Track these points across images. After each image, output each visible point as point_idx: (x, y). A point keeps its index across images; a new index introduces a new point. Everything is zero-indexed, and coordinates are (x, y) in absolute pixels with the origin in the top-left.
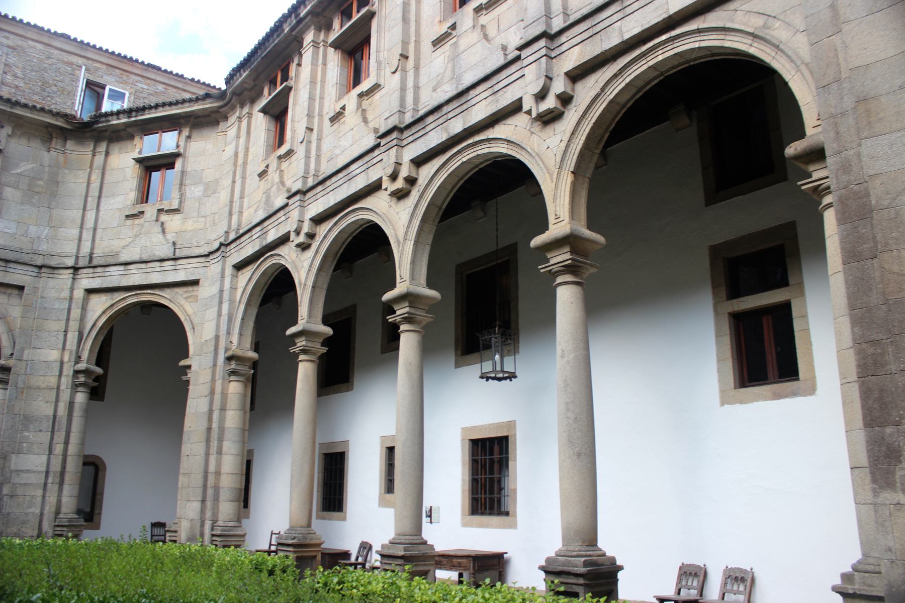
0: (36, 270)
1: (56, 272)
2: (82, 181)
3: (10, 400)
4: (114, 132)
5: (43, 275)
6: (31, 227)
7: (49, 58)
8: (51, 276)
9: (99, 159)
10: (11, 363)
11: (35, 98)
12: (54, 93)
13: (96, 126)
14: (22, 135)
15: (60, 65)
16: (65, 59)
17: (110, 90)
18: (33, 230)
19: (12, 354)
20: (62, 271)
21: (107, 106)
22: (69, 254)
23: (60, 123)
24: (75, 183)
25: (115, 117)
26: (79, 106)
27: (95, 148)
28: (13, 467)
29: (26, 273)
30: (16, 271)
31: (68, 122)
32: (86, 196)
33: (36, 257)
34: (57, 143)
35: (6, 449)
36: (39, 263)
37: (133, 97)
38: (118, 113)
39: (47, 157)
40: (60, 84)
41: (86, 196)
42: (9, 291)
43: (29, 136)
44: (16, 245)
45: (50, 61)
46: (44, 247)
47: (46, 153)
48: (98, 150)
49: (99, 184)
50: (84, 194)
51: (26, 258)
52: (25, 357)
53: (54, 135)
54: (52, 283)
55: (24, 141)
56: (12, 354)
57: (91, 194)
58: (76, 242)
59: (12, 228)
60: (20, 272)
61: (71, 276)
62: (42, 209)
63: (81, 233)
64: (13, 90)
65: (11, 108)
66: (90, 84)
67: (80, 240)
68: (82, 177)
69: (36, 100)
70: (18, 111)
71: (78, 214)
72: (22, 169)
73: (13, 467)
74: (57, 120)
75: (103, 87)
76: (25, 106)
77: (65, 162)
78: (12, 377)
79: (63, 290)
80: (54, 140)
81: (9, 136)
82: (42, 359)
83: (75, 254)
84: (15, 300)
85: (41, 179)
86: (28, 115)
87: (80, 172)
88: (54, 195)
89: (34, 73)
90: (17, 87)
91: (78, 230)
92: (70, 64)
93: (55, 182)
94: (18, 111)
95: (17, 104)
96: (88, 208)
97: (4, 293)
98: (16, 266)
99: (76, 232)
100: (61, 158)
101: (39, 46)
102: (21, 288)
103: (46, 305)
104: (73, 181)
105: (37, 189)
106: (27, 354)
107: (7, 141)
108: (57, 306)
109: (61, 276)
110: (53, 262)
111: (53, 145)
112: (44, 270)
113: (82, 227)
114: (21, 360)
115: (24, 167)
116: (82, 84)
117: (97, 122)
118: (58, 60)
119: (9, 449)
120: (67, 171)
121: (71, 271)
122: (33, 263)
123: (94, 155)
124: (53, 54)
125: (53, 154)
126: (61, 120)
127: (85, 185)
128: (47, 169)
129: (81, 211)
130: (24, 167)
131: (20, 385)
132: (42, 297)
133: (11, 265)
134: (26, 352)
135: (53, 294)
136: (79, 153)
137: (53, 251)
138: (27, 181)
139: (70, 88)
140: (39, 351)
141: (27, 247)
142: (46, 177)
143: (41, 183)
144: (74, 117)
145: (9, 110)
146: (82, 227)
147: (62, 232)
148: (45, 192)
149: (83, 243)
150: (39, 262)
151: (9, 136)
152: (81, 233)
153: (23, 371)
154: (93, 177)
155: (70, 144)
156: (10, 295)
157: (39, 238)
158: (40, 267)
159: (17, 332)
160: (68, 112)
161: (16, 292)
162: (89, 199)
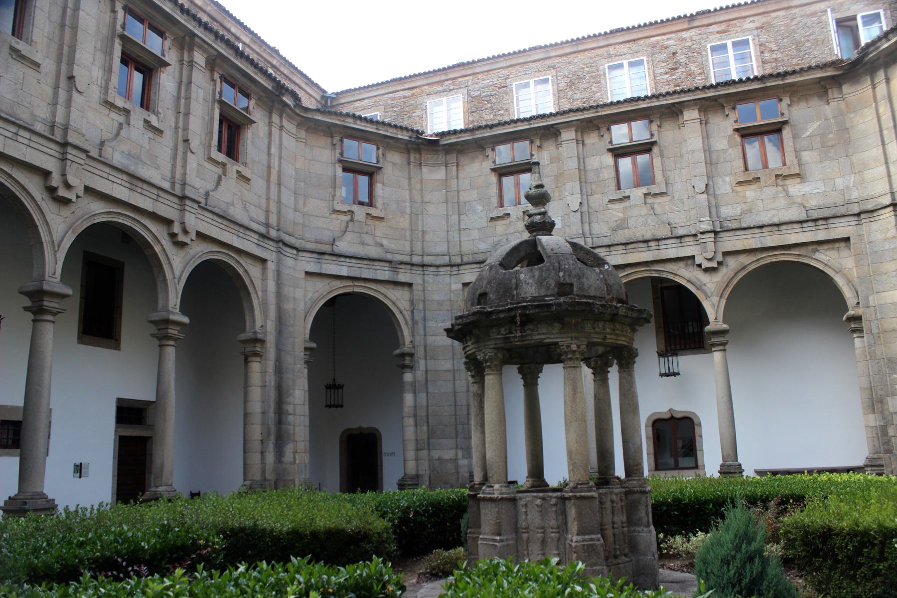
0: (856, 218)
1: (875, 214)
2: (871, 118)
3: (870, 346)
4: (887, 56)
5: (863, 221)
6: (837, 180)
7: (793, 19)
8: (871, 219)
9: (881, 89)
10: (860, 311)
11: (795, 61)
12: (810, 48)
13: (866, 59)
14: (799, 100)
15: (805, 20)
16: (808, 12)
17: (863, 17)
18: (840, 183)
19: (858, 303)
20: (881, 212)
21: (866, 35)
22: (883, 193)
23: (829, 73)
24: (865, 122)
25: (884, 40)
26: (837, 48)
27: (872, 81)
28: (891, 410)
29: (847, 224)
30: (837, 225)
31: (837, 69)
32: (881, 131)
33: (851, 206)
34: (833, 93)
35: (880, 392)
36: (856, 211)
37: (889, 12)
38: (886, 36)
39: (828, 110)
40: (811, 37)
41: (881, 131)
42: (837, 245)
43: (806, 97)
44: (828, 201)
45: (795, 22)
46: (855, 195)
47: (827, 107)
48: (876, 81)
49: (890, 114)
50: (877, 129)
51: (842, 211)
52: (871, 303)
53: (828, 87)
54: (874, 226)
55: (803, 105)
56: (858, 303)
57: (884, 126)
58: (886, 179)
59: (820, 187)
60: (841, 225)
61: (892, 213)
62: (842, 160)
63: (888, 168)
64: (774, 64)
65: (783, 80)
66: (840, 23)
67: (889, 176)
68: (869, 114)
69: (796, 63)
70: (790, 80)
71: (878, 152)
72: (811, 130)
73: (891, 410)
74: (826, 71)
75: (854, 18)
76: (794, 72)
77: (848, 106)
78: (864, 324)
79: (888, 229)
80: (830, 91)
81: (789, 105)
82: (889, 301)
83: (888, 191)
84: (844, 253)
85: (829, 133)
86: (799, 79)
87: (866, 110)
88: (847, 143)
89: (785, 40)
90: (776, 59)
91: (884, 167)
92: (814, 14)
93: (844, 130)
94: (790, 80)
95: (786, 74)
96: (886, 142)
97: (833, 248)
98: (836, 220)
99: (882, 169)
100: (843, 105)
101: (781, 13)
102: (847, 240)
103: (876, 249)
104: (861, 121)
105: (830, 143)
106: (873, 300)
107: (789, 111)
108: (887, 247)
109: (882, 217)
110: (870, 206)
111: (830, 96)
112: (862, 216)
113: (887, 163)
114: (868, 307)
115: (812, 128)
116: (832, 26)
117: (867, 55)
118: (802, 16)
119: (883, 393)
120: (852, 115)
121: (891, 209)
122: (850, 213)
123: (874, 88)
124: (795, 14)
125: (833, 104)
126: (830, 69)
127: (875, 120)
128: (832, 121)
129: (881, 147)
130: (812, 128)
131: (875, 330)
132: (870, 242)
133: (831, 221)
134: (871, 298)
135: (879, 236)
136: (857, 93)
137: (865, 195)
138: (818, 139)
139: (822, 37)
140: (883, 294)
141: (839, 200)
142: (834, 128)
143: (831, 136)
144: (841, 61)
145: (781, 83)
146: (887, 163)
147: (869, 174)
148: (840, 141)
149: (893, 178)
150: (856, 209)
151: (789, 105)
152: (888, 168)
153: (873, 316)
154: (881, 110)
155: (846, 88)
156: (838, 249)
157: (848, 188)
158: (858, 215)
159: (856, 281)
160: (829, 59)
161: (843, 245)
162: (885, 132)
